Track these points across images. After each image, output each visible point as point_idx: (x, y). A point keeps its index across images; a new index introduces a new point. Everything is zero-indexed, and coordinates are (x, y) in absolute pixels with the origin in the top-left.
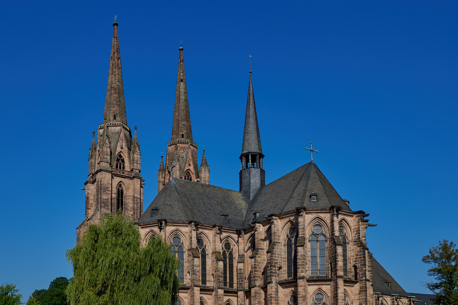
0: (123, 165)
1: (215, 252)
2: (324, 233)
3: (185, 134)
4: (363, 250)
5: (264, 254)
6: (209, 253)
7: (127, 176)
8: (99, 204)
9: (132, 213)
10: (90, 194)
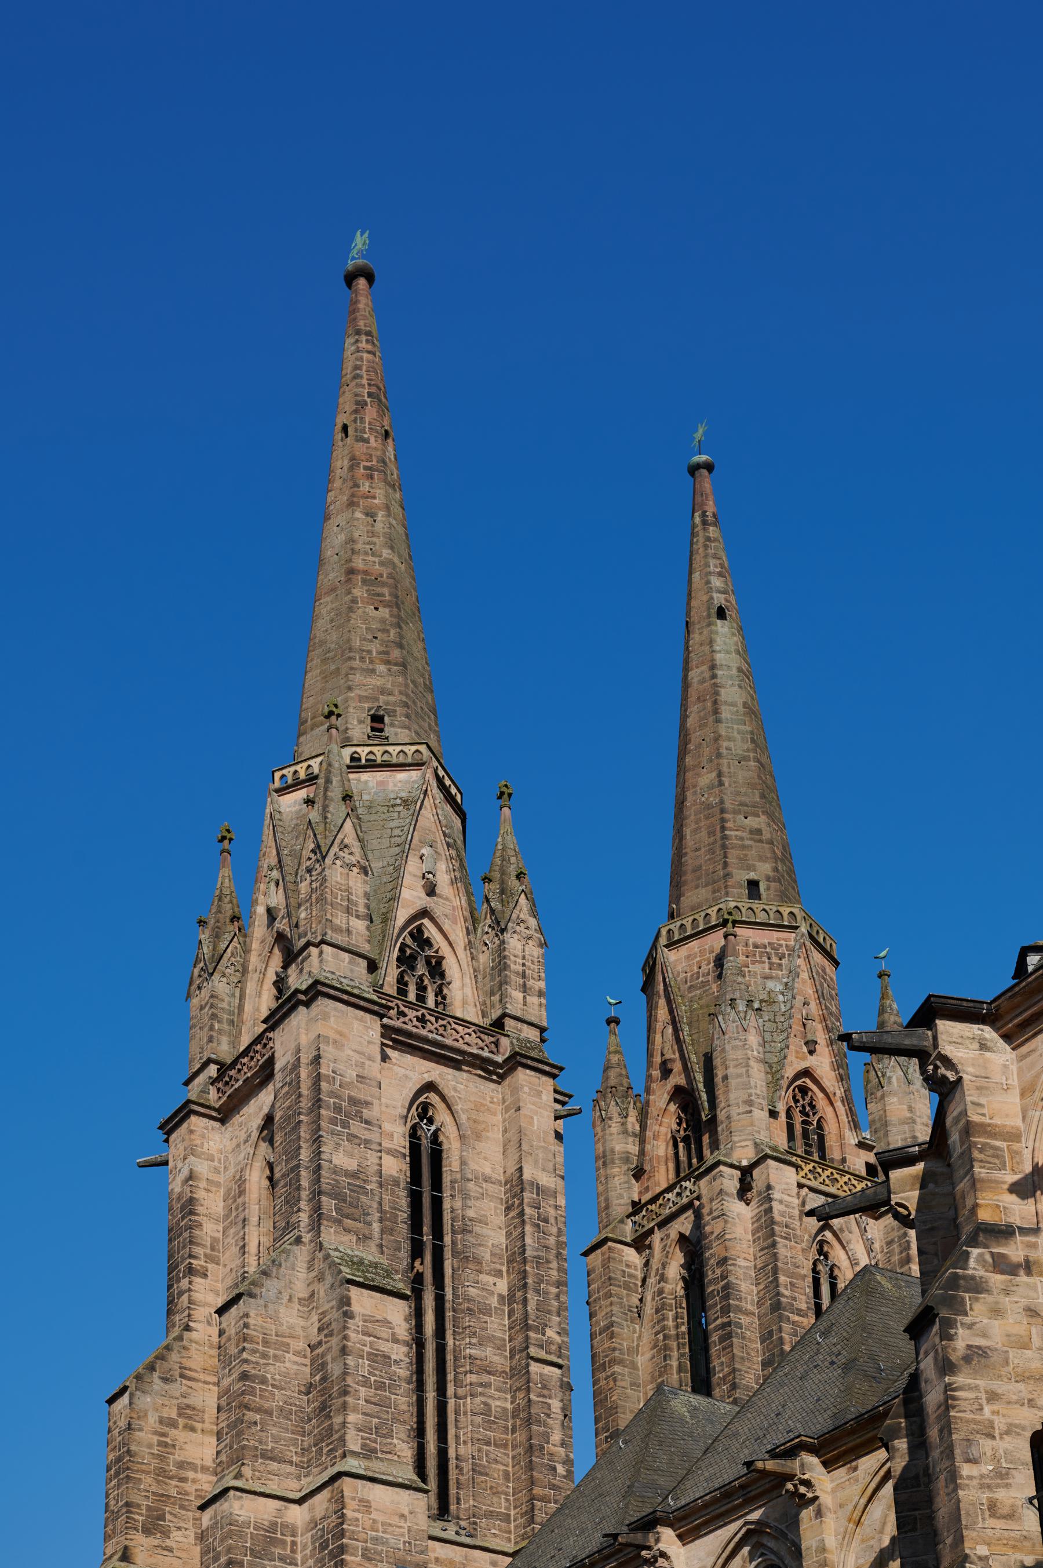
0: (439, 992)
3: (768, 879)
7: (471, 1054)
8: (303, 1204)
9: (502, 1286)
10: (203, 1184)
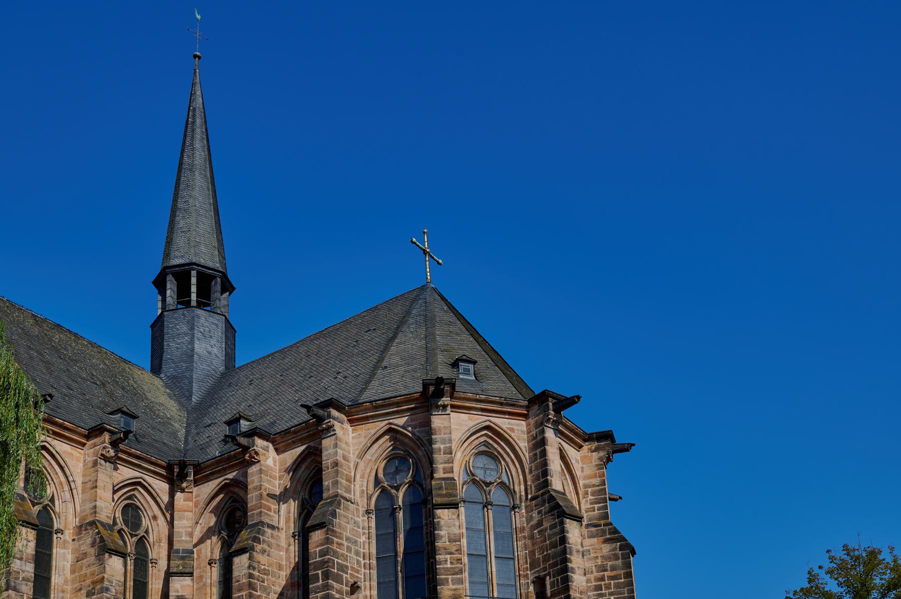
1: (93, 524)
2: (505, 479)
4: (622, 554)
5: (279, 545)
6: (65, 527)
